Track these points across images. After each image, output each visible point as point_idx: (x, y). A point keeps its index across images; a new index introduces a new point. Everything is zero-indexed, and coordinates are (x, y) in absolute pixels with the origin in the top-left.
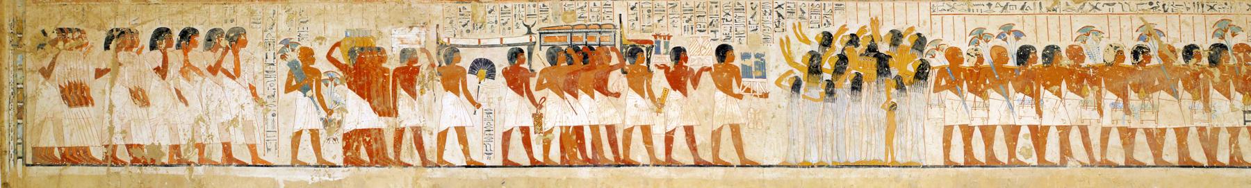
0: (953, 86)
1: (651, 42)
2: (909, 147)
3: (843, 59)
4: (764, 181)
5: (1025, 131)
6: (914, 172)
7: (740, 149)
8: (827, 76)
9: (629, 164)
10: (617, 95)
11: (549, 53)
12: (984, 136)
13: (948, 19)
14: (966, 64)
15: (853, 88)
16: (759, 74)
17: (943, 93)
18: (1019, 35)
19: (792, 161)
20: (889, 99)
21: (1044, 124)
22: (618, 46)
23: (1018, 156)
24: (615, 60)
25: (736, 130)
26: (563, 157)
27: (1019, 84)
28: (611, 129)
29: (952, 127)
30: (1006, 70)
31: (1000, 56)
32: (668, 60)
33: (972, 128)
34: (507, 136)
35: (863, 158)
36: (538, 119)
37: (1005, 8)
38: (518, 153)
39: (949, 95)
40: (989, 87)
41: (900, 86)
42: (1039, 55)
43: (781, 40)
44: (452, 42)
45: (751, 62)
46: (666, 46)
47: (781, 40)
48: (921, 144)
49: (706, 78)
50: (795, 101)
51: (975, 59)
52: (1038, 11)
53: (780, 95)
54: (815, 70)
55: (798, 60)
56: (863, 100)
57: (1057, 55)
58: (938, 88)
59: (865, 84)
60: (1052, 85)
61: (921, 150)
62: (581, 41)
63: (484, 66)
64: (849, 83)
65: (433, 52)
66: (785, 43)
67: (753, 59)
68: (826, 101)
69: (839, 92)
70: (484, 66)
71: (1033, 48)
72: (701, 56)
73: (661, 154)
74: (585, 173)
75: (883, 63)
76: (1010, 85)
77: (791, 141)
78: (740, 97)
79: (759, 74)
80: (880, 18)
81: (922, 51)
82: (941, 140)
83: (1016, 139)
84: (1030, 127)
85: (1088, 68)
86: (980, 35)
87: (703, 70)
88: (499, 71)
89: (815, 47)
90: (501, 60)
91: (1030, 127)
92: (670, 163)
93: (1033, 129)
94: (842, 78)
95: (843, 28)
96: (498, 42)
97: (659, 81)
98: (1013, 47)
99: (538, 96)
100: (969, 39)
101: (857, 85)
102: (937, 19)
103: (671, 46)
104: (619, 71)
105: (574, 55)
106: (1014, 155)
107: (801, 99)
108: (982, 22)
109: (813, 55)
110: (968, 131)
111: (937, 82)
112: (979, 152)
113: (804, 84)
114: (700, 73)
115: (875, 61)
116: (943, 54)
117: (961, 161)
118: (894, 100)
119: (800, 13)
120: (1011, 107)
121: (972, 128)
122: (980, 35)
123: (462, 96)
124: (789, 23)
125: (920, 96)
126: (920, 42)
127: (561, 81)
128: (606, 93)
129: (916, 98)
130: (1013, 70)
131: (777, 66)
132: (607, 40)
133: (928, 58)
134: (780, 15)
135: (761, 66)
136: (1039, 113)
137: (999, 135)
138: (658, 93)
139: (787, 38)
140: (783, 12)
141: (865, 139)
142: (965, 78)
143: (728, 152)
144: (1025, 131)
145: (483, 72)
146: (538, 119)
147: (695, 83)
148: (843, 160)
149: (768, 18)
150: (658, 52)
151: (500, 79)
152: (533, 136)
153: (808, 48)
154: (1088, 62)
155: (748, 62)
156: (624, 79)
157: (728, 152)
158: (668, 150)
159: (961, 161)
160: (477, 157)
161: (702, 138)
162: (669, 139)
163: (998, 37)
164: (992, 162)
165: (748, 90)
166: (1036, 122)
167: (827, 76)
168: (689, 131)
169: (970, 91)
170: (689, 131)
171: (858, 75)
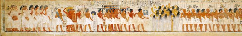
0: (184, 16)
1: (126, 8)
2: (176, 28)
3: (163, 11)
5: (198, 25)
7: (143, 29)
8: (160, 15)
9: (122, 31)
10: (119, 18)
11: (106, 10)
13: (183, 4)
15: (165, 17)
16: (147, 14)
17: (182, 18)
18: (197, 7)
19: (153, 31)
22: (120, 9)
23: (197, 30)
24: (119, 12)
25: (142, 25)
26: (109, 30)
27: (197, 16)
28: (118, 25)
30: (195, 13)
31: (193, 11)
32: (129, 12)
33: (188, 24)
34: (98, 26)
36: (104, 23)
38: (100, 29)
39: (183, 18)
41: (174, 17)
44: (88, 8)
45: (145, 12)
46: (129, 9)
48: (178, 28)
49: (137, 15)
53: (151, 18)
54: (158, 13)
55: (154, 11)
58: (181, 17)
59: (167, 16)
62: (112, 8)
63: (94, 13)
64: (164, 16)
65: (84, 10)
66: (152, 8)
67: (146, 11)
69: (162, 18)
70: (94, 13)
72: (136, 11)
73: (128, 29)
74: (113, 33)
75: (171, 12)
77: (153, 27)
78: (143, 18)
79: (147, 14)
83: (196, 27)
84: (199, 24)
86: (189, 7)
87: (136, 13)
88: (97, 14)
89: (158, 9)
90: (97, 12)
92: (130, 31)
95: (163, 6)
96: (96, 8)
97: (128, 16)
98: (196, 9)
99: (104, 18)
101: (166, 16)
103: (130, 9)
104: (120, 14)
105: (111, 11)
108: (190, 4)
109: (157, 11)
110: (187, 25)
112: (189, 29)
113: (155, 16)
114: (135, 14)
115: (169, 12)
120: (195, 20)
121: (188, 24)
123: (89, 18)
124: (152, 5)
125: (178, 18)
126: (178, 8)
127: (109, 15)
128: (117, 18)
129: (177, 19)
130: (196, 13)
131: (150, 12)
132: (117, 8)
133: (179, 11)
135: (147, 13)
137: (193, 26)
138: (127, 18)
140: (151, 2)
143: (141, 29)
144: (198, 25)
145: (94, 14)
146: (104, 23)
147: (134, 16)
148: (163, 31)
150: (127, 10)
151: (97, 15)
152: (103, 26)
153: (156, 9)
155: (144, 12)
156: (121, 15)
157: (141, 29)
158: (129, 29)
160: (92, 30)
161: (136, 26)
162: (129, 27)
165: (145, 17)
168: (133, 25)
169: (188, 17)
170: (133, 25)
171: (166, 14)
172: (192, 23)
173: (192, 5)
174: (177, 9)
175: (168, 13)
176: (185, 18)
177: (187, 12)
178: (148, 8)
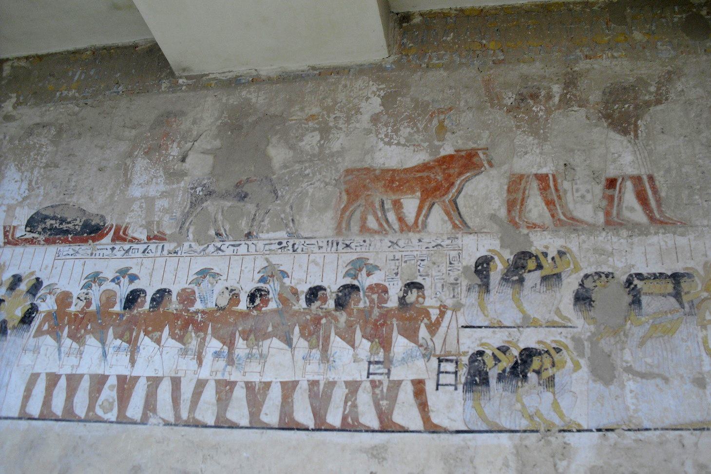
5: (112, 381)
12: (68, 385)
14: (73, 309)
18: (133, 278)
21: (133, 374)
27: (120, 330)
30: (112, 314)
37: (127, 251)
39: (49, 340)
42: (148, 299)
57: (166, 298)
58: (39, 333)
60: (153, 331)
76: (111, 331)
80: (7, 263)
81: (34, 295)
82: (23, 388)
83: (99, 391)
85: (197, 313)
93: (122, 379)
98: (124, 289)
100: (83, 282)
102: (59, 263)
106: (94, 411)
111: (40, 327)
116: (54, 298)
120: (105, 354)
122: (96, 278)
130: (118, 314)
133: (37, 302)
136: (133, 361)
137: (85, 384)
142: (69, 323)
154: (198, 306)
163: (113, 280)
166: (125, 371)
172: (79, 371)
176: (58, 339)
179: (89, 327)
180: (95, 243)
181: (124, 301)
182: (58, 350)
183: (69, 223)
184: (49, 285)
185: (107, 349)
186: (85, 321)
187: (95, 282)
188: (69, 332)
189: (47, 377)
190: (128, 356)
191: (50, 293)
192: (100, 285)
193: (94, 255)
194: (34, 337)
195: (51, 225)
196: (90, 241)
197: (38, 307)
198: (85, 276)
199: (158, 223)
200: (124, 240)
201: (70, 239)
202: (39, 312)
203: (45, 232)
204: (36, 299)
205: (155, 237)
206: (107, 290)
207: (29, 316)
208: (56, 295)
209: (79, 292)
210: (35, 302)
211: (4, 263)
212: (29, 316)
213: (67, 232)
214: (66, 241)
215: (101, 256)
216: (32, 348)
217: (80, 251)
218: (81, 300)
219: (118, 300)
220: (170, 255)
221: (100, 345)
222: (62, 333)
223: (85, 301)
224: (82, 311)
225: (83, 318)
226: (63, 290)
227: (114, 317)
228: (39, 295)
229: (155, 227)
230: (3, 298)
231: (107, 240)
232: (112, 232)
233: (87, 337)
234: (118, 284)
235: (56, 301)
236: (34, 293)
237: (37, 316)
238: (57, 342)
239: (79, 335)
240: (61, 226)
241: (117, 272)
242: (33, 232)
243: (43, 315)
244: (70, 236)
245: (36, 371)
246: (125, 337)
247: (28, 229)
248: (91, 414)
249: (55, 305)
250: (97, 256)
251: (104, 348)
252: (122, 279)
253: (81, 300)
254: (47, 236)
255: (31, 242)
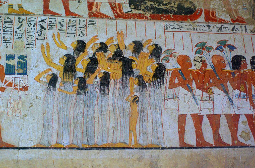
3: (94, 62)
4: (18, 162)
5: (243, 119)
6: (155, 153)
12: (211, 123)
13: (178, 35)
14: (193, 68)
16: (21, 71)
17: (177, 89)
18: (232, 48)
19: (46, 144)
20: (132, 93)
23: (239, 138)
27: (236, 83)
29: (185, 116)
31: (220, 62)
35: (110, 141)
37: (220, 29)
39: (182, 90)
40: (213, 85)
41: (142, 83)
42: (248, 62)
43: (42, 46)
47: (42, 46)
48: (160, 130)
50: (51, 93)
51: (200, 65)
52: (244, 32)
54: (69, 67)
55: (56, 61)
56: (110, 94)
58: (172, 85)
59: (112, 81)
61: (160, 135)
64: (98, 79)
67: (17, 60)
68: (78, 93)
69: (90, 88)
71: (244, 57)
75: (127, 67)
76: (229, 84)
77: (46, 126)
79: (21, 71)
80: (125, 32)
81: (158, 57)
82: (176, 126)
83: (236, 125)
84: (247, 116)
86: (202, 47)
89: (71, 52)
91: (247, 116)
94: (93, 76)
95: (95, 38)
98: (228, 56)
100: (195, 49)
101: (105, 81)
106: (237, 139)
107: (57, 92)
108: (204, 38)
109: (69, 57)
110: (198, 119)
113: (60, 80)
115: (120, 64)
116: (175, 60)
117: (194, 144)
118: (137, 94)
119: (59, 26)
120: (231, 100)
121: (202, 116)
124: (49, 33)
125: (158, 91)
129: (153, 94)
130: (230, 73)
133: (163, 62)
134: (42, 27)
135: (23, 67)
137: (223, 122)
139: (48, 44)
140: (45, 25)
141: (112, 125)
142: (194, 78)
144: (243, 119)
148: (92, 143)
149: (31, 29)
153: (65, 53)
155: (11, 62)
159: (194, 144)
163: (217, 49)
164: (219, 144)
165: (10, 84)
167: (80, 74)
169: (198, 88)
171: (106, 74)
172: (216, 112)
173: (212, 40)
174: (151, 55)
175: (115, 69)
176: (190, 89)
177: (196, 67)
178: (29, 45)
179: (211, 81)
180: (193, 21)
181: (231, 64)
182: (193, 97)
183: (166, 5)
184: (168, 50)
185: (230, 96)
186: (207, 76)
187: (204, 50)
188: (196, 84)
189: (192, 118)
190: (249, 101)
191: (171, 56)
192: (209, 52)
193: (196, 30)
194: (169, 88)
195: (151, 5)
196: (189, 20)
197: (165, 67)
198: (194, 44)
199: (236, 11)
200: (215, 21)
201: (171, 17)
202: (167, 70)
203: (148, 10)
204: (161, 60)
205: (237, 20)
206: (215, 55)
207: (160, 73)
208: (176, 57)
209: (194, 56)
210: (160, 62)
211: (122, 32)
212: (160, 73)
213: (167, 11)
214: (168, 18)
215: (202, 31)
216: (172, 96)
217: (183, 26)
218: (198, 62)
219: (227, 63)
220: (252, 33)
221: (224, 94)
222: (192, 85)
223: (201, 63)
224: (201, 69)
225: (204, 74)
226: (181, 54)
227: (228, 74)
228: (162, 57)
229: (234, 14)
230: (132, 59)
231: (202, 19)
232: (203, 14)
233: (213, 88)
234: (222, 51)
235: (178, 62)
236: (157, 55)
237: (166, 72)
238: (190, 92)
239: (206, 87)
240: (160, 7)
241: (218, 43)
242: (138, 10)
243: (171, 72)
244: (171, 15)
245: (182, 112)
246: (242, 88)
247: (132, 7)
248: (236, 142)
249: (179, 65)
250: (199, 31)
251: (228, 96)
252: (223, 48)
253: (198, 62)
254: (151, 13)
255: (135, 17)
